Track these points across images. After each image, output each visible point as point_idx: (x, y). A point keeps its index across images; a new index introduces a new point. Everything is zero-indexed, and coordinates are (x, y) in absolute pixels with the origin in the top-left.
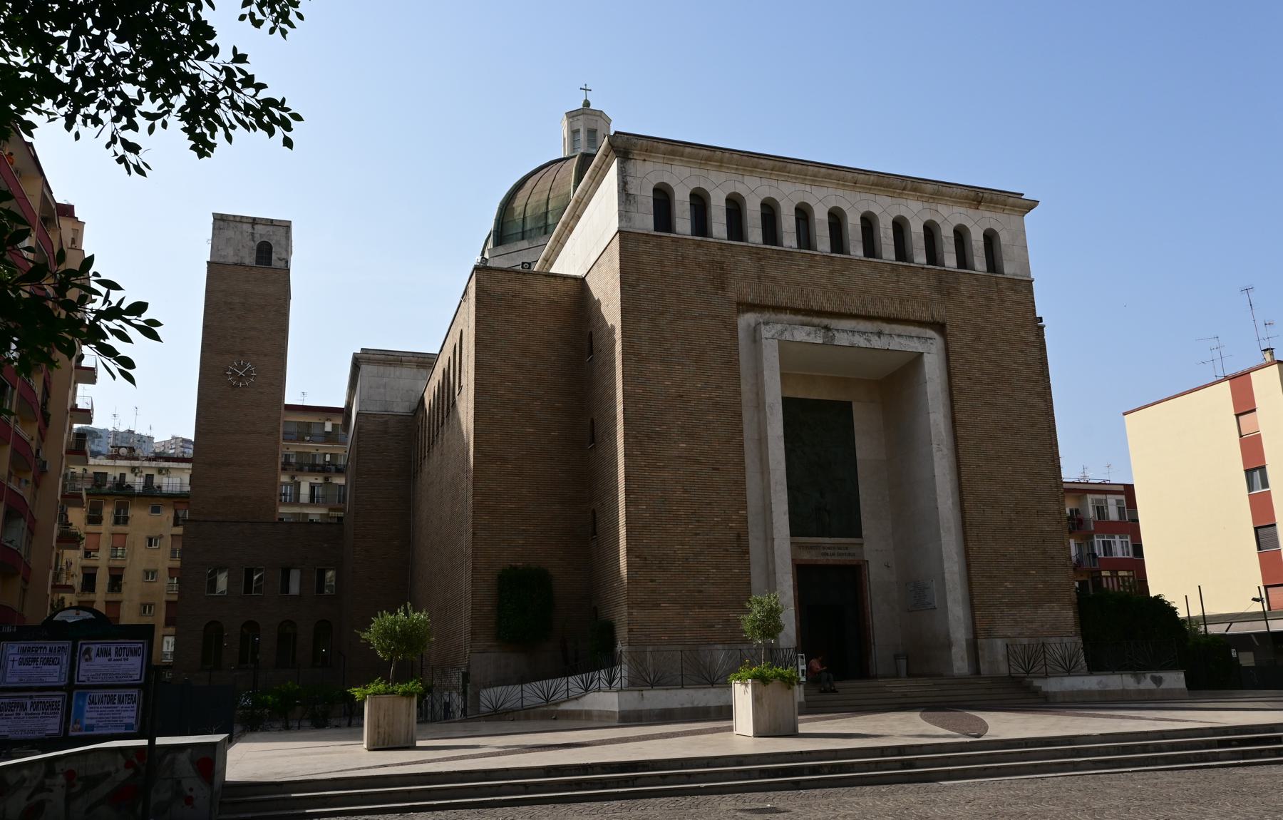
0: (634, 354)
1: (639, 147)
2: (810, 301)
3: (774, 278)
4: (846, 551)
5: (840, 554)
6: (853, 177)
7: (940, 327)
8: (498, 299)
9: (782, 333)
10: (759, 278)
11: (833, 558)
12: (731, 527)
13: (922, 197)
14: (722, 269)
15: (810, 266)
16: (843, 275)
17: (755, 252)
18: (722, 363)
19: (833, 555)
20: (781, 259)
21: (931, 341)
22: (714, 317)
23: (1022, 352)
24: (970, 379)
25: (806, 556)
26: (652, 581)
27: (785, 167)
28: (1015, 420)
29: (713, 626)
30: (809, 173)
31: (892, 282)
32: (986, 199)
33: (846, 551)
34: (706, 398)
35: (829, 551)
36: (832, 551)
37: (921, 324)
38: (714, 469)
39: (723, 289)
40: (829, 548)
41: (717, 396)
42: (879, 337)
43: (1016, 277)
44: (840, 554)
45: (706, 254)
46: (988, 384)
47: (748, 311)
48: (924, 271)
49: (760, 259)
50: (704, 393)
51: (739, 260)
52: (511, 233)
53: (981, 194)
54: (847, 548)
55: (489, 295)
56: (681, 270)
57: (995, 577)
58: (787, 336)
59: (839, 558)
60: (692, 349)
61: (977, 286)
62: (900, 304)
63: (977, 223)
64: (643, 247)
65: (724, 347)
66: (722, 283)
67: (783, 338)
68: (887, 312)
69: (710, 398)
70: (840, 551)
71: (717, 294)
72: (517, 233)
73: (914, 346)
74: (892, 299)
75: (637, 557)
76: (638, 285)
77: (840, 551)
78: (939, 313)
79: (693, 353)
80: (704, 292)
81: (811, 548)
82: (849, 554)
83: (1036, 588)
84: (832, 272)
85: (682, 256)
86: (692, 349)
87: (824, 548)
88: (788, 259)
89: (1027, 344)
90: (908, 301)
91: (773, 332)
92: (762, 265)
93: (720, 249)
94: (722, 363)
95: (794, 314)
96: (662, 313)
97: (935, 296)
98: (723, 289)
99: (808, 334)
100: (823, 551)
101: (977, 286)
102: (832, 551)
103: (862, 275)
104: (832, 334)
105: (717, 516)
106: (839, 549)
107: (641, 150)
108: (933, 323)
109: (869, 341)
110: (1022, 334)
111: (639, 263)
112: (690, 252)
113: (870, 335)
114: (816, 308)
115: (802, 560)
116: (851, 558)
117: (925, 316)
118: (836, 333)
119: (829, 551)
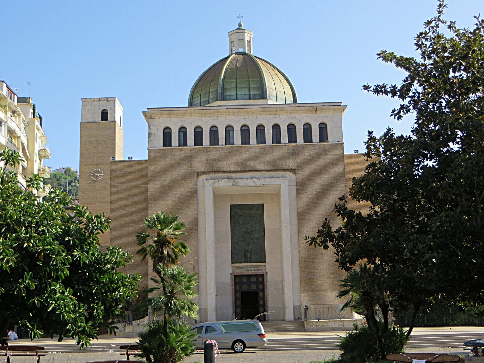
0: (153, 198)
1: (155, 114)
2: (230, 167)
3: (214, 159)
4: (258, 269)
6: (251, 110)
7: (293, 171)
8: (120, 173)
9: (214, 183)
10: (207, 160)
11: (252, 271)
12: (191, 264)
14: (191, 158)
15: (231, 152)
16: (246, 154)
17: (207, 150)
18: (189, 198)
19: (252, 270)
20: (217, 151)
21: (285, 178)
22: (186, 179)
23: (335, 177)
24: (306, 193)
25: (239, 272)
27: (219, 111)
28: (328, 209)
30: (230, 112)
31: (270, 154)
32: (318, 109)
33: (258, 269)
34: (182, 213)
35: (250, 269)
36: (251, 269)
37: (284, 170)
39: (191, 167)
40: (250, 268)
41: (187, 212)
42: (260, 180)
43: (334, 143)
45: (184, 153)
46: (316, 194)
47: (203, 174)
48: (286, 146)
49: (207, 152)
50: (181, 211)
51: (198, 154)
52: (195, 103)
53: (315, 107)
54: (258, 267)
55: (116, 172)
56: (173, 162)
57: (312, 279)
59: (254, 271)
60: (177, 194)
61: (313, 149)
62: (273, 163)
63: (322, 117)
64: (158, 154)
65: (190, 191)
66: (191, 164)
67: (214, 186)
68: (266, 168)
69: (184, 213)
70: (255, 269)
71: (188, 169)
72: (198, 103)
74: (269, 161)
76: (155, 170)
77: (255, 269)
78: (292, 164)
79: (177, 195)
80: (183, 170)
82: (259, 270)
83: (333, 283)
84: (240, 153)
85: (173, 156)
86: (177, 194)
88: (220, 150)
89: (338, 174)
90: (277, 161)
91: (210, 183)
92: (208, 155)
93: (191, 150)
94: (189, 198)
95: (224, 173)
96: (165, 180)
97: (291, 157)
98: (191, 167)
99: (226, 182)
100: (247, 269)
101: (313, 149)
102: (251, 269)
103: (255, 152)
104: (237, 181)
105: (185, 260)
106: (254, 267)
107: (156, 115)
110: (336, 169)
111: (156, 161)
112: (177, 154)
113: (255, 179)
114: (232, 170)
115: (237, 273)
116: (260, 271)
117: (285, 167)
118: (239, 180)
119: (250, 269)
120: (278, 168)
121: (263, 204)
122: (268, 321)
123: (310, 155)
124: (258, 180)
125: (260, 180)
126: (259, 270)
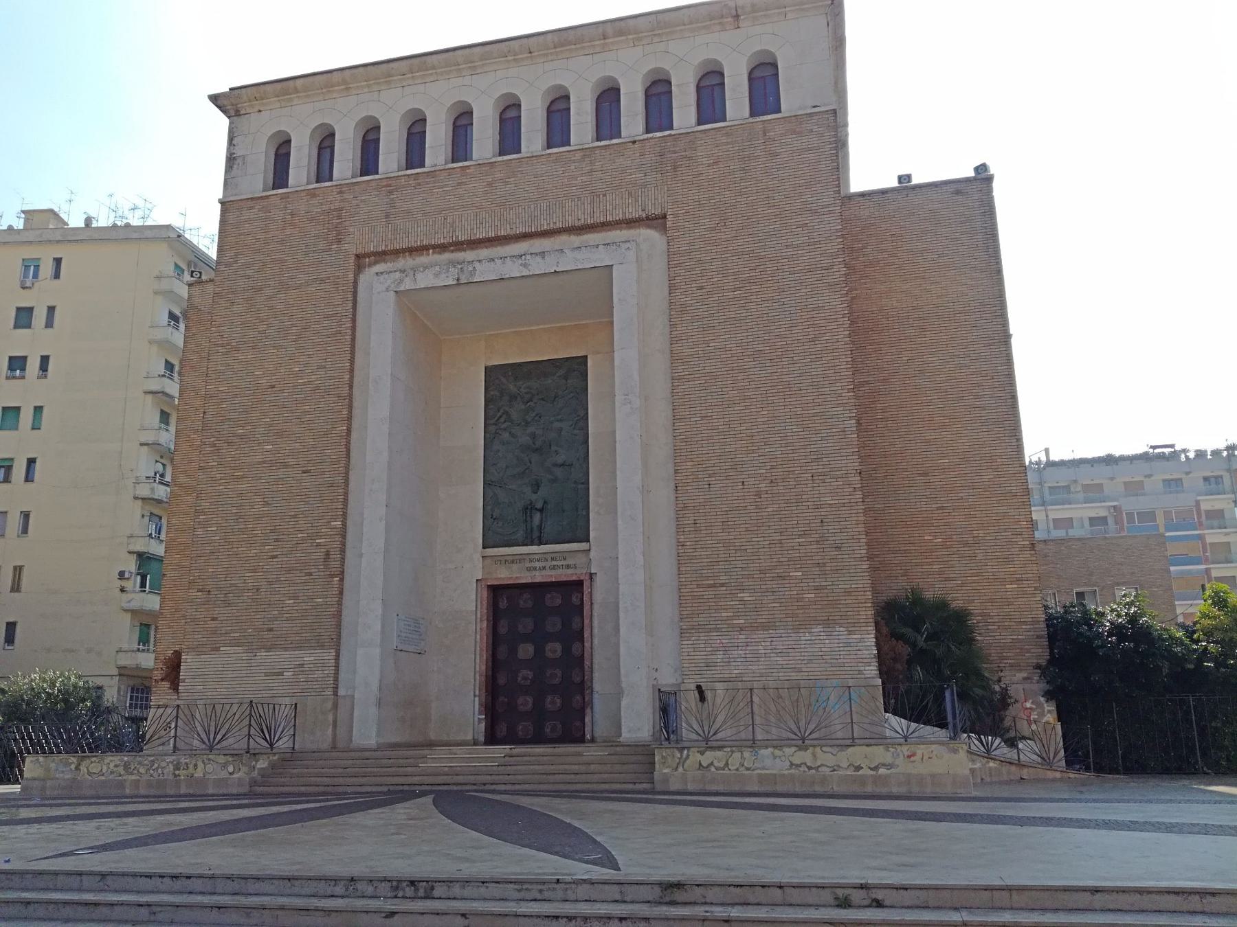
0: (222, 345)
1: (245, 98)
4: (564, 563)
5: (554, 568)
7: (657, 221)
9: (401, 281)
11: (544, 572)
12: (319, 544)
13: (640, 39)
14: (340, 217)
15: (460, 184)
17: (390, 187)
19: (544, 568)
21: (628, 245)
22: (322, 281)
24: (701, 288)
25: (504, 575)
26: (213, 619)
28: (780, 336)
29: (281, 674)
33: (564, 563)
34: (304, 384)
35: (537, 564)
37: (631, 223)
38: (304, 472)
39: (339, 242)
40: (538, 560)
42: (543, 258)
44: (554, 568)
46: (735, 289)
49: (391, 192)
55: (200, 310)
56: (288, 232)
57: (722, 585)
58: (408, 284)
59: (553, 573)
61: (728, 143)
62: (592, 202)
65: (332, 316)
66: (339, 234)
67: (402, 288)
68: (570, 221)
69: (310, 383)
70: (554, 563)
71: (330, 250)
73: (601, 258)
75: (199, 590)
76: (236, 262)
77: (554, 563)
81: (513, 562)
82: (568, 567)
87: (531, 561)
90: (604, 195)
91: (389, 282)
92: (392, 199)
93: (340, 192)
96: (261, 290)
99: (436, 275)
100: (528, 565)
101: (728, 143)
104: (471, 269)
106: (552, 559)
108: (648, 218)
109: (525, 266)
113: (528, 257)
116: (570, 571)
117: (633, 212)
118: (477, 265)
119: (537, 564)
120: (609, 218)
121: (586, 357)
122: (593, 740)
123: (716, 163)
124: (538, 259)
125: (543, 258)
126: (568, 567)
